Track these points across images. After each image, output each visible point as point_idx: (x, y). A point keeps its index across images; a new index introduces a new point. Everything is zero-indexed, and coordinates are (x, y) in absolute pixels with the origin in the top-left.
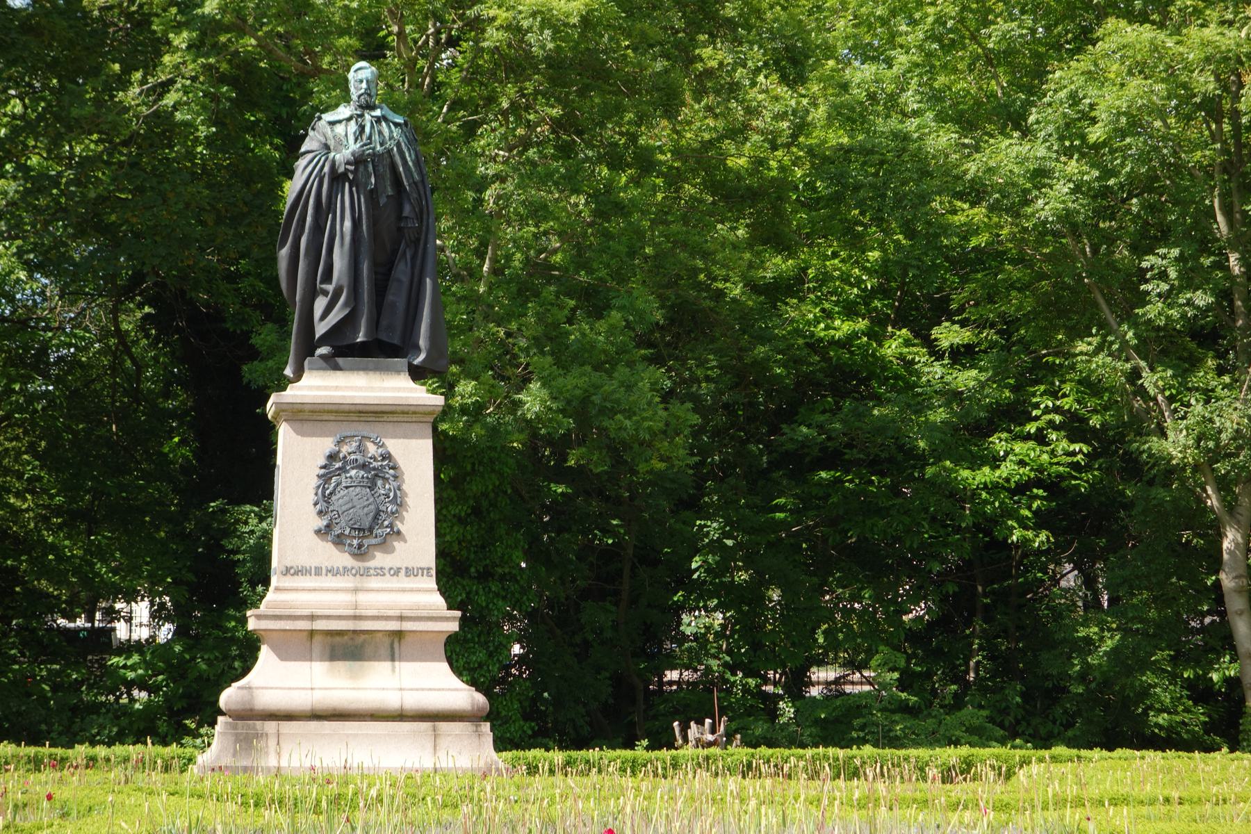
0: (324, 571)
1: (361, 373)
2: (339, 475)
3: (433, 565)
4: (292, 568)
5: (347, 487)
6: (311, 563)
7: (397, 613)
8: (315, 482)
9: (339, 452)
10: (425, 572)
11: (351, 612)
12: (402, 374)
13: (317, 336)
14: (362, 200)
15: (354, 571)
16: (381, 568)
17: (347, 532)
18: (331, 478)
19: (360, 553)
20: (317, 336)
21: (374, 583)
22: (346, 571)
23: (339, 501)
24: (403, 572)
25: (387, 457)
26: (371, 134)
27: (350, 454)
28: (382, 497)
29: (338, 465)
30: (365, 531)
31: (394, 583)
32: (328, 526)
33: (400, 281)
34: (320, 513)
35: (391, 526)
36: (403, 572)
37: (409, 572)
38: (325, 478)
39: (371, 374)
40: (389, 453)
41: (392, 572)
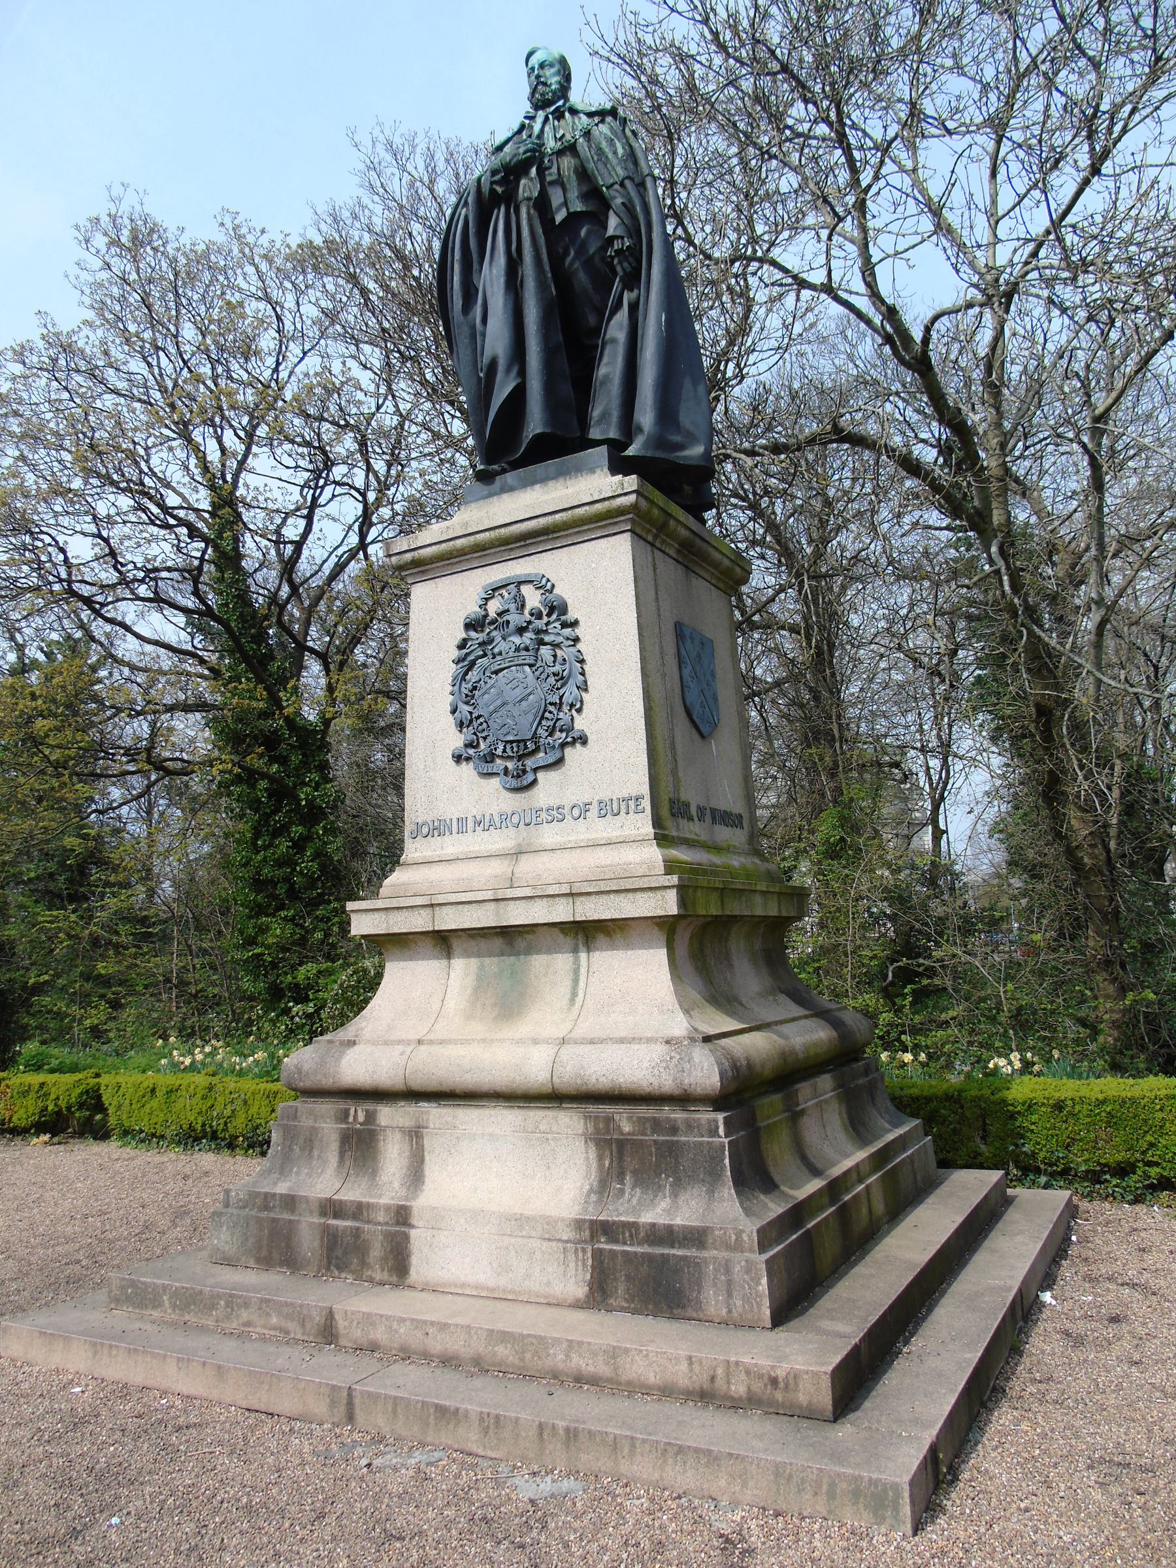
0: (470, 824)
1: (537, 487)
3: (645, 790)
5: (496, 672)
6: (450, 811)
7: (565, 889)
8: (451, 669)
10: (632, 804)
12: (598, 471)
15: (515, 819)
17: (499, 752)
18: (472, 664)
19: (522, 783)
21: (549, 835)
22: (505, 818)
23: (486, 702)
24: (594, 810)
25: (557, 608)
26: (542, 131)
30: (523, 749)
31: (581, 831)
33: (614, 341)
34: (461, 725)
35: (569, 729)
36: (594, 810)
37: (607, 809)
38: (466, 664)
39: (551, 484)
41: (576, 812)
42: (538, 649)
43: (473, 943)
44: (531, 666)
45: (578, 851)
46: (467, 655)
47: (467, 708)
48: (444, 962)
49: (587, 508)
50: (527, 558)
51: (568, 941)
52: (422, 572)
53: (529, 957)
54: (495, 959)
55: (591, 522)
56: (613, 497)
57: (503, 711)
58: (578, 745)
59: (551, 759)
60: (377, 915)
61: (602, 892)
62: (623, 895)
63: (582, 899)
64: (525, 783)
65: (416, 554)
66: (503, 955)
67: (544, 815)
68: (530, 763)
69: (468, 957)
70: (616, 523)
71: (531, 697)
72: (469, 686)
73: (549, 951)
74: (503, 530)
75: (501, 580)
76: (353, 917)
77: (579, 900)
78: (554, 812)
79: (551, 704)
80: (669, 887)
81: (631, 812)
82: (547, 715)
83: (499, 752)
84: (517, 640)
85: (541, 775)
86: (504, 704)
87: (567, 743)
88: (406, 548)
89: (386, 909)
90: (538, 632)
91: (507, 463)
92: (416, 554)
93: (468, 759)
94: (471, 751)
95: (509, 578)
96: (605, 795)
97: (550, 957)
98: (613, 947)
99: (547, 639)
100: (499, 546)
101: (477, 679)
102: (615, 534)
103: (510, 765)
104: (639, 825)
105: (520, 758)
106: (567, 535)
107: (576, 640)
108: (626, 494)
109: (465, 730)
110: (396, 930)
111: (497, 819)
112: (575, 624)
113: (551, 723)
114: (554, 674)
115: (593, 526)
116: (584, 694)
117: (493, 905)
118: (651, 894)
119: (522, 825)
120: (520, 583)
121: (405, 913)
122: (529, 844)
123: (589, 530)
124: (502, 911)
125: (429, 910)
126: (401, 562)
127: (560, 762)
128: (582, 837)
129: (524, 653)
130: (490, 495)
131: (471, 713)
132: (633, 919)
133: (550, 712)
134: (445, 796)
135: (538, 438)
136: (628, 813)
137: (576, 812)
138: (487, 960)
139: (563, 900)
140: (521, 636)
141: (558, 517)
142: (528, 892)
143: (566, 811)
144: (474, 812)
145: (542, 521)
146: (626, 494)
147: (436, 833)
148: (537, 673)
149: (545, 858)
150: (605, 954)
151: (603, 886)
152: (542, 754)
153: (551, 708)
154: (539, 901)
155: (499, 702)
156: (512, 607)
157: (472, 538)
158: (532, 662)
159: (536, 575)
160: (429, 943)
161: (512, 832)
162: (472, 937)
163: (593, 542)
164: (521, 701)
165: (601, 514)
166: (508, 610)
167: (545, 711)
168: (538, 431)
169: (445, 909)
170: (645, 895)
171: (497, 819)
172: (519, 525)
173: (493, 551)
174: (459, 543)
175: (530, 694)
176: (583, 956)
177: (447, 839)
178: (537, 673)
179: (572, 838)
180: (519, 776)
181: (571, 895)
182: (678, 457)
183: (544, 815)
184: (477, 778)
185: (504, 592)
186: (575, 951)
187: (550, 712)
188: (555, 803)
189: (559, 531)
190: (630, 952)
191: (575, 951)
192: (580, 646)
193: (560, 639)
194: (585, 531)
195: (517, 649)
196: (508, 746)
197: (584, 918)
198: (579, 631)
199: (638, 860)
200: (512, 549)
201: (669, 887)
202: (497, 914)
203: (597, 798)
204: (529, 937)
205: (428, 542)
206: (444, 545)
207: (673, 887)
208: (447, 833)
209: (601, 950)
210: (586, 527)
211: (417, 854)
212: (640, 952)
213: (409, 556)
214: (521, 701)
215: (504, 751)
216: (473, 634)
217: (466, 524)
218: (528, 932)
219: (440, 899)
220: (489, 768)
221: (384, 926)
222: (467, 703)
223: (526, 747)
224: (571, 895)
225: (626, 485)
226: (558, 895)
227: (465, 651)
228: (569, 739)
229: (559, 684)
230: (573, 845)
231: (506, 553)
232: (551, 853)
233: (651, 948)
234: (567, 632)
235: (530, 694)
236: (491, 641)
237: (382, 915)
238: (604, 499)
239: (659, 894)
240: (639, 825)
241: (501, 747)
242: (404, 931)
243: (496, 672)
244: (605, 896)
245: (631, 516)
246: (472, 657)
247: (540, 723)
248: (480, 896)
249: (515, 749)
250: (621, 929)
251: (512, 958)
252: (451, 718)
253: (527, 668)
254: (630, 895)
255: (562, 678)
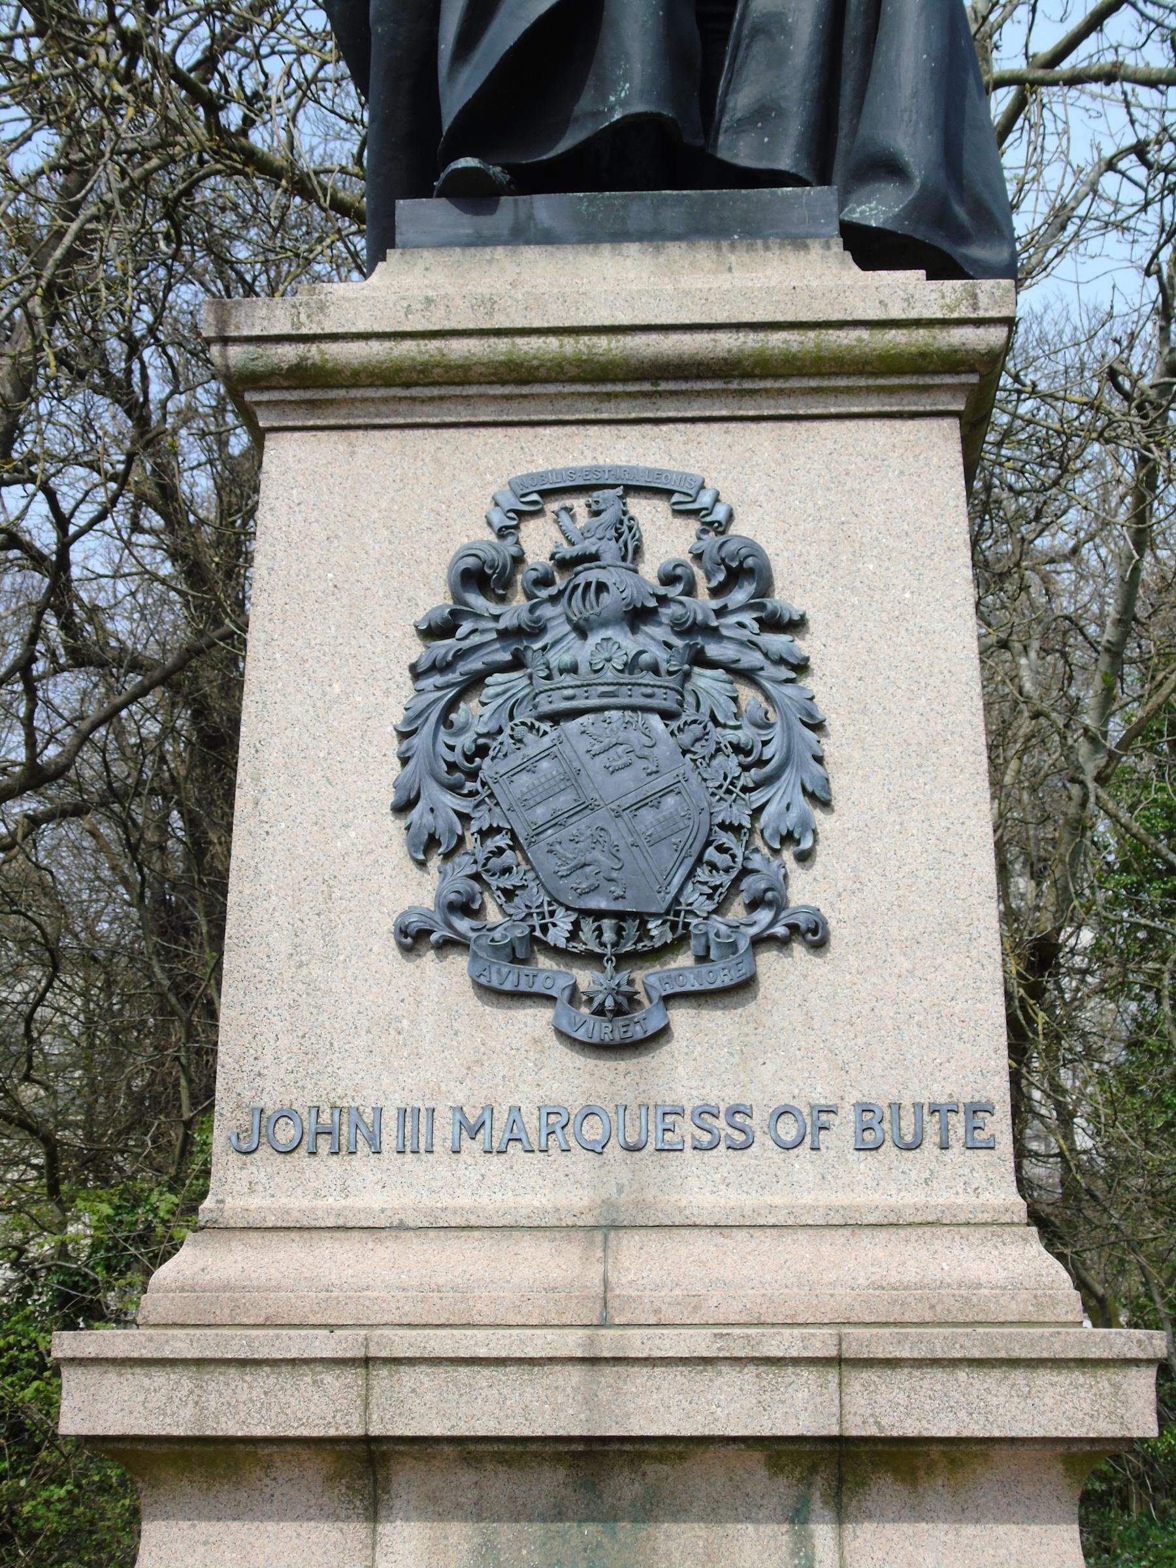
0: (445, 1129)
1: (633, 248)
2: (517, 663)
4: (287, 1114)
5: (555, 718)
7: (821, 1344)
9: (518, 560)
10: (958, 1122)
11: (572, 1343)
12: (816, 248)
13: (447, 122)
14: (735, 24)
15: (593, 1130)
16: (735, 1111)
17: (558, 936)
18: (475, 682)
20: (447, 122)
24: (844, 1127)
27: (565, 564)
28: (732, 764)
29: (516, 609)
32: (465, 908)
39: (675, 250)
40: (755, 551)
41: (788, 1130)
42: (687, 676)
43: (467, 1477)
44: (667, 715)
45: (802, 1235)
46: (461, 655)
47: (451, 801)
48: (357, 1530)
49: (864, 334)
50: (648, 429)
51: (783, 1488)
52: (312, 404)
53: (648, 1529)
54: (536, 1529)
55: (861, 373)
56: (945, 323)
57: (580, 825)
58: (798, 949)
59: (721, 975)
60: (160, 1379)
61: (935, 1362)
62: (997, 1373)
63: (866, 1375)
64: (638, 1032)
65: (313, 351)
66: (559, 1515)
67: (686, 1128)
68: (646, 978)
69: (441, 1516)
70: (926, 389)
71: (670, 801)
72: (465, 742)
73: (714, 1514)
74: (603, 343)
75: (572, 472)
76: (71, 1379)
77: (858, 1380)
78: (721, 1123)
79: (723, 826)
80: (1136, 1362)
81: (957, 1147)
82: (711, 854)
83: (558, 936)
84: (627, 643)
85: (681, 1018)
86: (584, 807)
87: (773, 939)
88: (284, 329)
89: (200, 1362)
90: (689, 629)
91: (507, 168)
92: (313, 351)
93: (446, 946)
94: (463, 925)
95: (596, 470)
96: (881, 1093)
97: (719, 1530)
98: (917, 1513)
99: (713, 650)
100: (573, 380)
101: (493, 726)
102: (914, 415)
103: (585, 978)
104: (978, 1179)
105: (623, 960)
106: (781, 392)
107: (801, 668)
108: (979, 322)
109: (435, 862)
110: (230, 1427)
111: (531, 1121)
112: (796, 626)
113: (725, 879)
114: (737, 749)
115: (863, 382)
116: (818, 815)
117: (576, 1375)
118: (1078, 1377)
119: (614, 1151)
120: (631, 490)
121: (266, 1379)
122: (640, 1205)
123: (848, 390)
124: (604, 1395)
125: (352, 1377)
126: (259, 367)
127: (745, 987)
128: (807, 1199)
129: (649, 678)
130: (480, 241)
131: (464, 818)
132: (1013, 1441)
133: (721, 849)
134: (362, 1041)
135: (632, 123)
136: (944, 1147)
137: (788, 1130)
138: (506, 1531)
139: (807, 1375)
140: (634, 629)
141: (777, 340)
142: (700, 1343)
143: (756, 1123)
144: (460, 1096)
145: (727, 342)
146: (979, 322)
147: (324, 1144)
148: (686, 738)
149: (700, 1245)
150: (890, 1530)
151: (939, 1343)
152: (684, 960)
153: (726, 839)
154: (730, 1374)
155: (565, 801)
156: (610, 550)
157: (502, 345)
158: (671, 704)
159: (684, 476)
160: (316, 1467)
161: (581, 1162)
162: (503, 1459)
163: (851, 424)
164: (641, 804)
165: (899, 356)
166: (594, 557)
167: (708, 843)
168: (639, 108)
169: (409, 1377)
170: (1063, 1379)
171: (531, 1121)
172: (653, 338)
173: (552, 389)
174: (459, 348)
175: (666, 791)
176: (823, 1533)
177: (363, 1165)
178: (686, 738)
179: (777, 1200)
180: (618, 1011)
181: (838, 1362)
182: (966, 257)
183: (686, 1128)
184: (471, 1002)
185: (579, 504)
186: (798, 1516)
187: (721, 849)
188: (722, 1095)
189: (763, 377)
190: (969, 1530)
191: (798, 1516)
192: (809, 684)
193: (751, 659)
194: (791, 392)
195: (631, 666)
196: (588, 926)
197: (872, 1431)
198: (803, 646)
199: (1000, 1276)
200: (609, 396)
201: (1136, 1362)
202: (590, 1401)
203: (854, 1096)
204: (653, 1470)
205: (360, 327)
206: (408, 348)
207: (1149, 1362)
208: (363, 1148)
209: (882, 1518)
210: (842, 382)
211: (254, 1202)
212: (1001, 1529)
213: (288, 354)
214: (641, 804)
215: (574, 935)
216: (477, 601)
217: (490, 304)
218: (660, 1459)
219: (403, 1343)
220: (508, 977)
221: (188, 1412)
222: (454, 788)
223: (644, 933)
224: (838, 1362)
225: (983, 300)
226: (796, 1361)
227: (445, 647)
228: (780, 930)
229: (748, 779)
230: (780, 1219)
231: (588, 404)
232: (716, 1236)
233: (1033, 1520)
234: (776, 642)
235: (666, 791)
236: (537, 630)
237: (185, 1380)
238: (918, 323)
239: (1104, 1380)
240: (978, 1179)
241: (563, 923)
242: (259, 1431)
243: (555, 718)
244: (940, 1374)
245: (974, 379)
246: (475, 664)
247: (691, 874)
248: (539, 1344)
249: (609, 936)
250: (954, 1464)
251: (589, 1529)
252: (394, 827)
253: (655, 721)
254: (1019, 1376)
255: (761, 763)
